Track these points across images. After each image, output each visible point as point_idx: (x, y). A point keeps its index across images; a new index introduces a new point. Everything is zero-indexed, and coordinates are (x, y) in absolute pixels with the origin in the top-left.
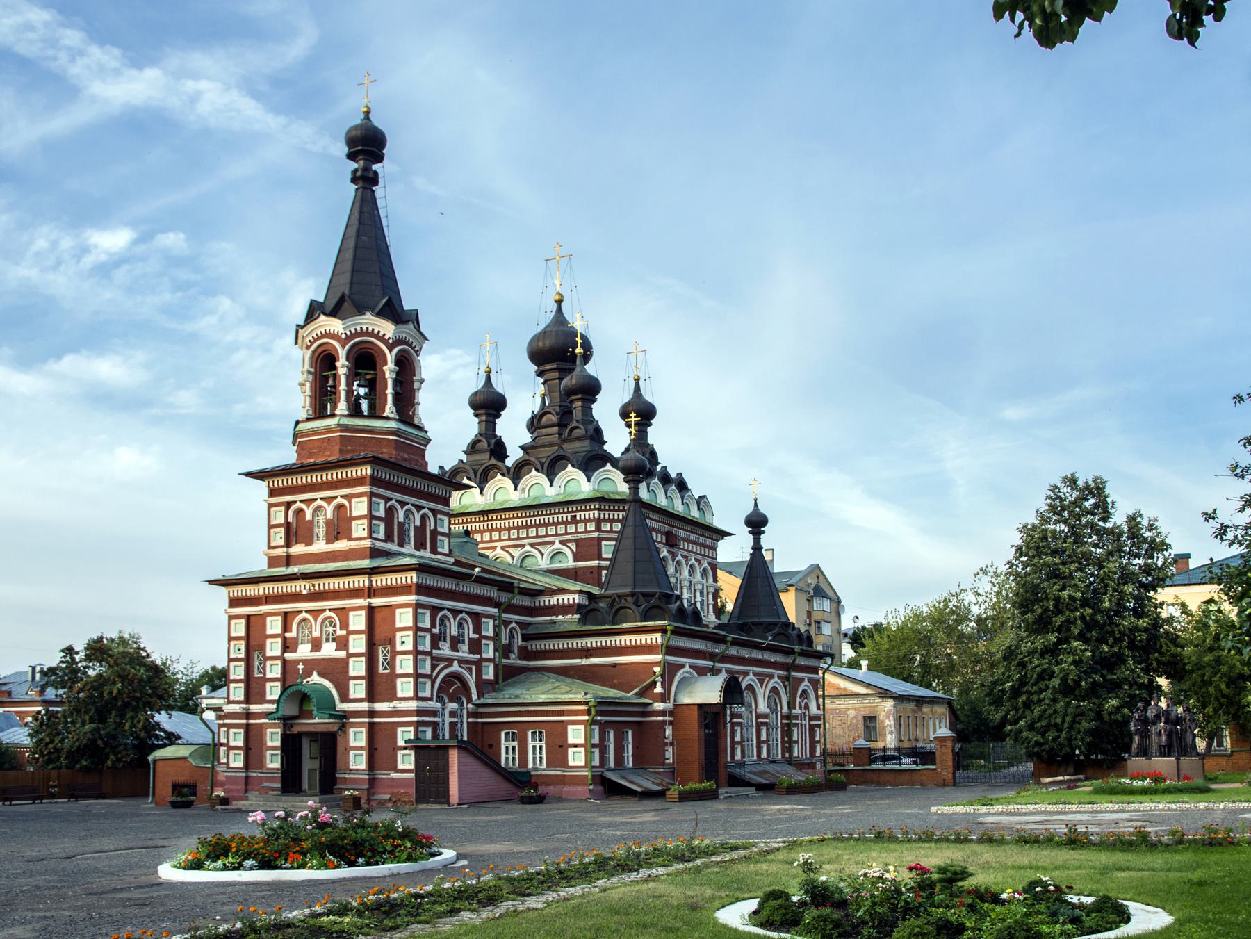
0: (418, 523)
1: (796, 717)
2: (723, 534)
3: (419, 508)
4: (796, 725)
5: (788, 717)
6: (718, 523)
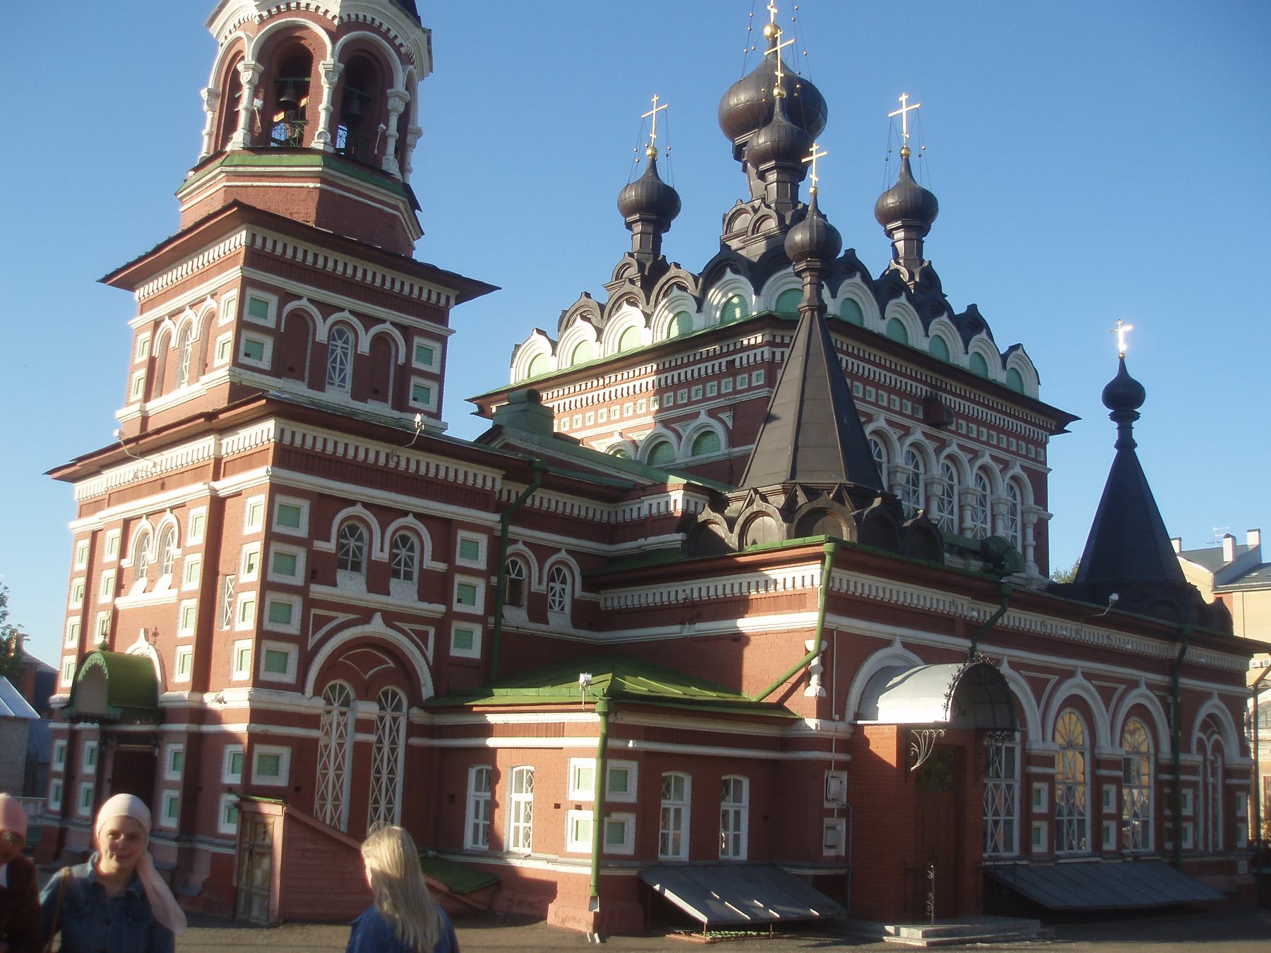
0: (364, 347)
1: (1192, 770)
2: (1059, 421)
3: (369, 321)
4: (1193, 785)
5: (1174, 768)
6: (1047, 395)
